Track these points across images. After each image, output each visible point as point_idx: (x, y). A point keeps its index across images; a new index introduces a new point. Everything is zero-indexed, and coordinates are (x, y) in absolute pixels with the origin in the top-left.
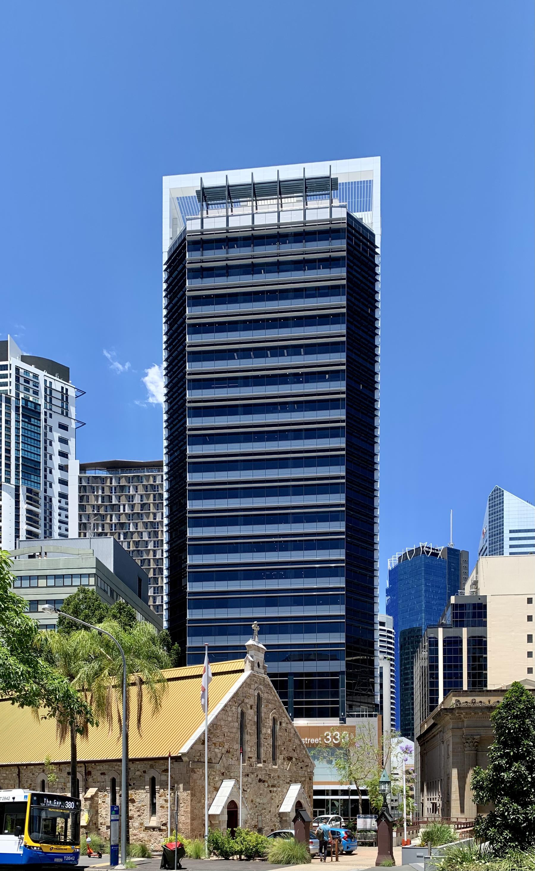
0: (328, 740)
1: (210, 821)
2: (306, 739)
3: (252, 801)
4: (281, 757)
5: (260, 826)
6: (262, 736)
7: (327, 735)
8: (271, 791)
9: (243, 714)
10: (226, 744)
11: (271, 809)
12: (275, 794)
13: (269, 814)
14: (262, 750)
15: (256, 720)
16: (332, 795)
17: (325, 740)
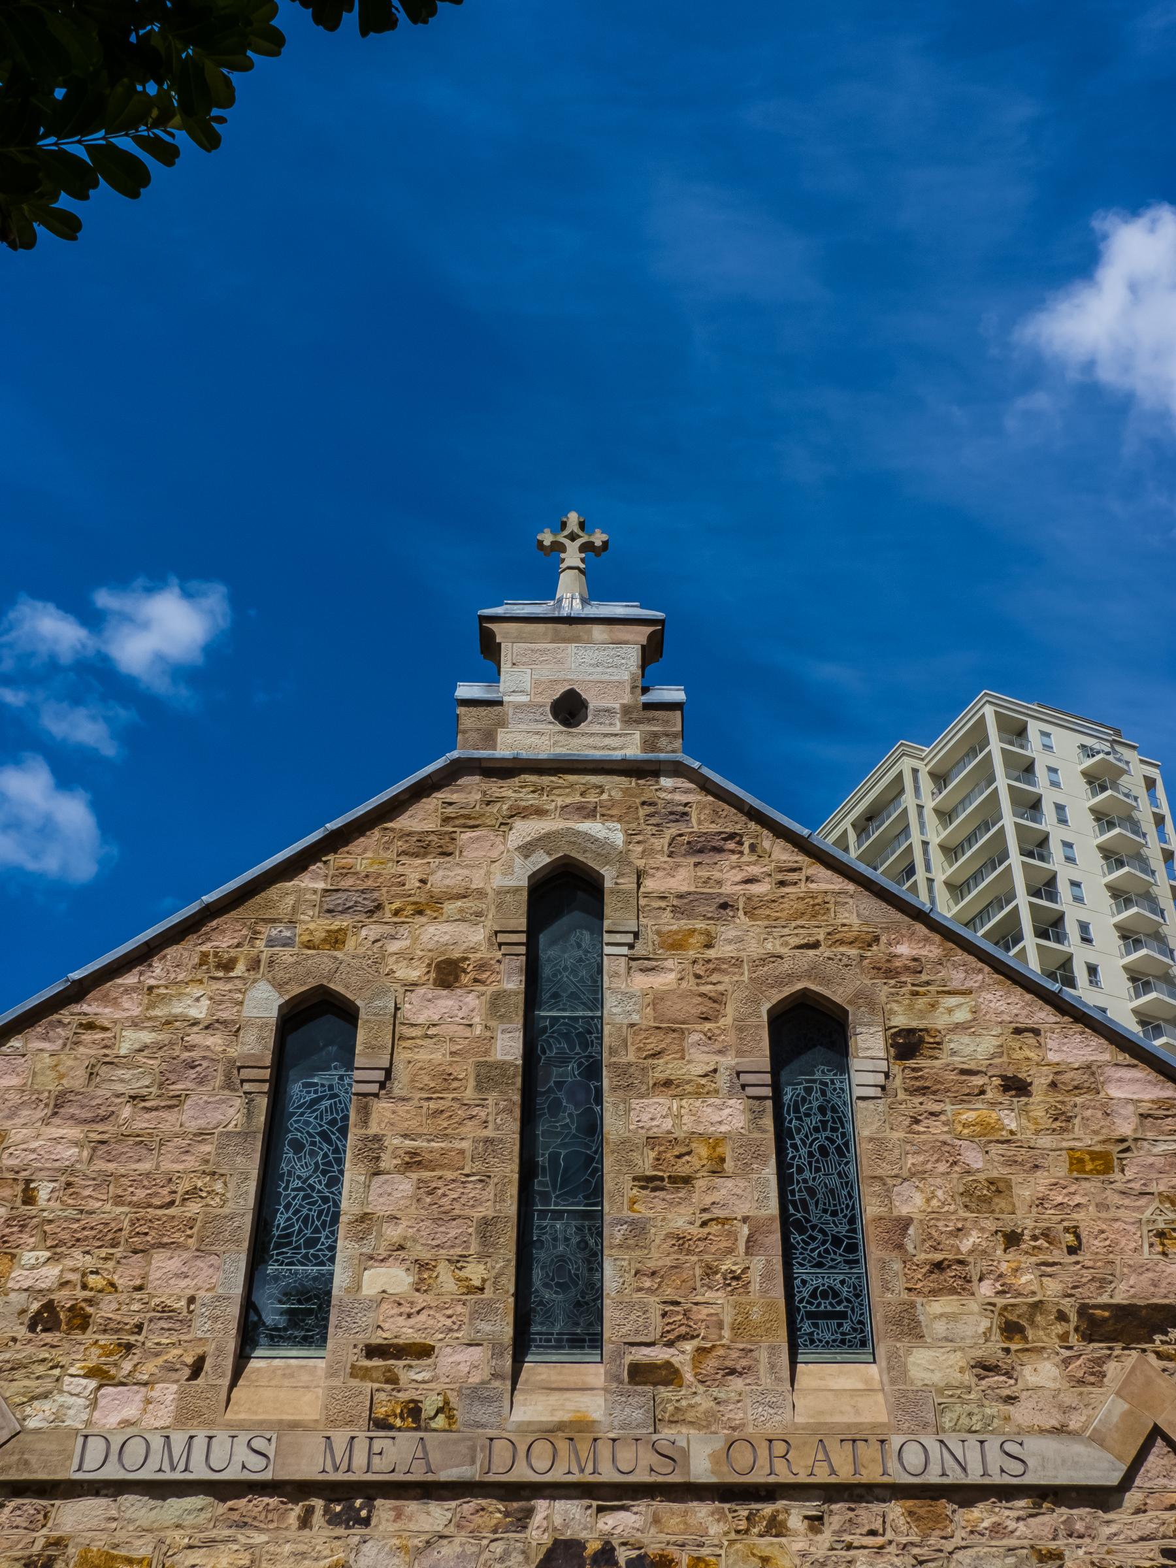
10: (28, 1257)
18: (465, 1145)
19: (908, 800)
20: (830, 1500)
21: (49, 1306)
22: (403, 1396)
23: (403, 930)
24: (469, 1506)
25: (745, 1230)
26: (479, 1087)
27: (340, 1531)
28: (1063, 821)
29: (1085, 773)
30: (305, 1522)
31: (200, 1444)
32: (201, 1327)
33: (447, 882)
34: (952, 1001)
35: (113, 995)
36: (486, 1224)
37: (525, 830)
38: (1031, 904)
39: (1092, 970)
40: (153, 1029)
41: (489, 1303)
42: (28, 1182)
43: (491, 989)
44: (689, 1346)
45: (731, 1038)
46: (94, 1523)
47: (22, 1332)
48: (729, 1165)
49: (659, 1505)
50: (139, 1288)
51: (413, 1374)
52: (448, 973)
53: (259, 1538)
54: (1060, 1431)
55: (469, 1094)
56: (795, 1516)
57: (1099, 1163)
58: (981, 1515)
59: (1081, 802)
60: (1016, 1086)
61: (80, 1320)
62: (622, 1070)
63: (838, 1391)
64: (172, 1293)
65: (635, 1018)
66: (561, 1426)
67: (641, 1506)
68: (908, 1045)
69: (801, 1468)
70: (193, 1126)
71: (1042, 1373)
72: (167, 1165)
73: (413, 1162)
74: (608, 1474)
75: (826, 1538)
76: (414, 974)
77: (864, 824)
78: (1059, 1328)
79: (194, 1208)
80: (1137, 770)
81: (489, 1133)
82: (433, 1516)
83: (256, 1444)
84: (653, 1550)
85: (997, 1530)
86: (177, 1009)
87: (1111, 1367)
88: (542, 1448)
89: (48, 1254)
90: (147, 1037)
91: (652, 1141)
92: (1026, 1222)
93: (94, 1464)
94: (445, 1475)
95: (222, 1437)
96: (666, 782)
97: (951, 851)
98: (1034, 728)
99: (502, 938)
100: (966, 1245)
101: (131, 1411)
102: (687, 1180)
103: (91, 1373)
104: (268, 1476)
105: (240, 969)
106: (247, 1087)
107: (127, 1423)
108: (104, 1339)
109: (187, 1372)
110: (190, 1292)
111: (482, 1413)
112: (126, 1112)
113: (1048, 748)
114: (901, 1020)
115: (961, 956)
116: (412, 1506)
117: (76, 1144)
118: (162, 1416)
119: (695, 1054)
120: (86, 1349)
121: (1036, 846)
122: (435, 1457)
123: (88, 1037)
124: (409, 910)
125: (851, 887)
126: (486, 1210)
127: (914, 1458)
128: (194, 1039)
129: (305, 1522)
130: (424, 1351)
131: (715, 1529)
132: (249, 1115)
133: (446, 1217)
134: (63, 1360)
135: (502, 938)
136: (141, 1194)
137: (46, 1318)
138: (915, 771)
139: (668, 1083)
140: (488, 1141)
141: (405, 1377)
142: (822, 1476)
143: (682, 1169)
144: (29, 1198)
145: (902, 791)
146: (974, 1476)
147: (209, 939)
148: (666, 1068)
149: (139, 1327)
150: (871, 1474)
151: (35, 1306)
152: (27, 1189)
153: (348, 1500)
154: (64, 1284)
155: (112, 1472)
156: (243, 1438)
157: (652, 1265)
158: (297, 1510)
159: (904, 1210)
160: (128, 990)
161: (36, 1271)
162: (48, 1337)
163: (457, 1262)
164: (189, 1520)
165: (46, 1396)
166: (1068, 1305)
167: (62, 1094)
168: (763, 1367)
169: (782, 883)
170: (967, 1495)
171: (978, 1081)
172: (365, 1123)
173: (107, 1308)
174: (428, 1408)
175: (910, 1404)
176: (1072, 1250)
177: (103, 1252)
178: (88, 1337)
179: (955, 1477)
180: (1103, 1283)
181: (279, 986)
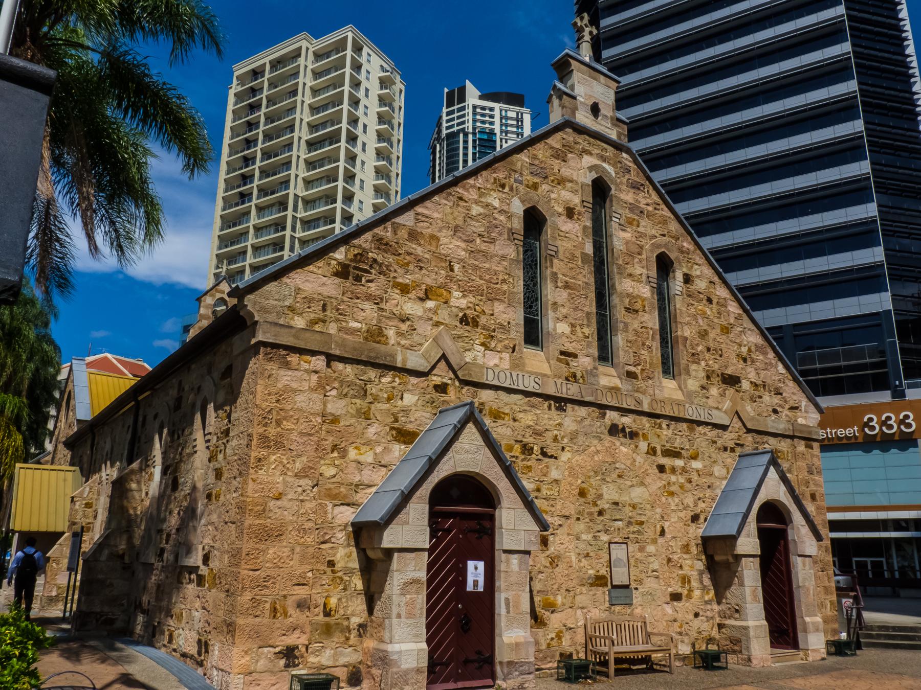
0: (873, 428)
1: (364, 550)
2: (829, 430)
3: (582, 493)
4: (698, 371)
5: (620, 576)
6: (618, 304)
7: (871, 420)
8: (661, 469)
9: (534, 221)
11: (666, 525)
12: (682, 480)
13: (661, 540)
14: (619, 340)
15: (589, 249)
16: (896, 530)
17: (866, 430)
18: (580, 283)
19: (301, 61)
20: (672, 420)
21: (465, 315)
22: (572, 370)
23: (555, 190)
24: (591, 409)
25: (651, 332)
26: (582, 262)
27: (559, 413)
28: (367, 96)
29: (380, 78)
30: (550, 408)
31: (520, 376)
32: (513, 334)
33: (566, 174)
34: (696, 267)
35: (467, 187)
36: (588, 314)
37: (588, 160)
38: (348, 129)
39: (363, 163)
40: (482, 207)
41: (591, 342)
42: (450, 262)
43: (583, 224)
44: (639, 367)
45: (644, 262)
46: (491, 399)
47: (458, 324)
48: (646, 308)
49: (635, 416)
50: (492, 315)
51: (573, 363)
52: (570, 213)
53: (539, 412)
54: (717, 408)
55: (580, 263)
56: (664, 423)
57: (726, 330)
58: (701, 429)
59: (376, 91)
60: (710, 301)
61: (476, 324)
62: (619, 266)
63: (669, 388)
64: (503, 318)
65: (621, 248)
66: (613, 388)
67: (631, 416)
68: (687, 279)
69: (668, 411)
70: (500, 253)
71: (714, 391)
72: (494, 268)
73: (567, 286)
74: (625, 406)
75: (670, 431)
76: (560, 210)
77: (276, 64)
78: (717, 379)
79: (505, 287)
80: (399, 85)
81: (586, 280)
82: (583, 411)
83: (537, 380)
84: (634, 429)
85: (705, 434)
86: (490, 200)
87: (727, 392)
88: (609, 394)
89: (461, 294)
90: (482, 210)
91: (628, 295)
92: (711, 345)
93: (491, 379)
94: (587, 399)
95: (526, 375)
96: (624, 155)
97: (315, 91)
98: (366, 50)
99: (585, 204)
100: (700, 348)
101: (496, 361)
102: (637, 311)
103: (483, 344)
104: (540, 391)
105: (507, 190)
106: (516, 241)
107: (496, 365)
108: (485, 332)
109: (511, 350)
110: (507, 320)
111: (593, 380)
112: (478, 241)
113: (369, 61)
114: (685, 270)
115: (698, 252)
116: (576, 407)
117: (464, 250)
118: (506, 365)
119: (636, 266)
120: (478, 336)
121: (355, 102)
122: (583, 393)
123: (462, 203)
124: (556, 182)
125: (672, 216)
126: (586, 309)
127: (690, 412)
128: (496, 215)
129: (550, 408)
130: (575, 356)
131: (647, 425)
132: (518, 253)
133: (576, 309)
134: (474, 338)
135: (585, 204)
136: (487, 277)
137: (464, 320)
138: (308, 49)
139: (631, 275)
140: (586, 283)
141: (572, 364)
142: (672, 414)
143: (636, 308)
144: (452, 270)
145: (299, 55)
146: (702, 419)
147: (495, 172)
148: (630, 269)
149: (494, 330)
150: (681, 416)
151: (461, 315)
152: (450, 265)
153: (560, 403)
154: (469, 308)
155: (496, 382)
156: (532, 377)
157: (630, 338)
158: (546, 404)
159: (686, 335)
160: (473, 186)
161: (459, 300)
162: (467, 328)
163: (581, 326)
164: (518, 403)
165: (469, 350)
166: (719, 372)
167: (456, 226)
168: (656, 378)
169: (655, 209)
170: (700, 423)
171: (702, 296)
172: (552, 266)
173: (483, 320)
174: (579, 375)
175: (689, 395)
176: (721, 356)
177: (480, 298)
178: (479, 330)
179: (699, 419)
180: (726, 367)
181: (523, 202)
